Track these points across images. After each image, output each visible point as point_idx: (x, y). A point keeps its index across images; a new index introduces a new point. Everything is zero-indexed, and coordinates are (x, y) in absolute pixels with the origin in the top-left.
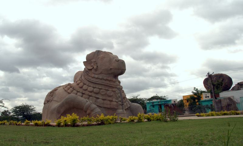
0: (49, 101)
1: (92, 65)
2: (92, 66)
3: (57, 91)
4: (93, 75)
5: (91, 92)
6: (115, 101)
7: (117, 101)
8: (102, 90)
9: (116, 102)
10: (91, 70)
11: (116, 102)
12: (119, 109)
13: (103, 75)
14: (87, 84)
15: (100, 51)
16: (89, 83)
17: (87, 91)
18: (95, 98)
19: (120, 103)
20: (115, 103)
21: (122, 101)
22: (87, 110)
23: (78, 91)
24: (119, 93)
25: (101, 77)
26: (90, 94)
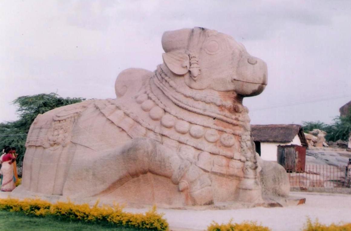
0: (58, 144)
1: (185, 65)
4: (189, 92)
5: (183, 133)
7: (243, 159)
8: (209, 131)
9: (240, 160)
10: (182, 76)
11: (240, 160)
12: (244, 177)
16: (178, 109)
17: (173, 129)
18: (193, 150)
20: (240, 164)
22: (180, 180)
23: (150, 127)
24: (248, 140)
26: (183, 138)
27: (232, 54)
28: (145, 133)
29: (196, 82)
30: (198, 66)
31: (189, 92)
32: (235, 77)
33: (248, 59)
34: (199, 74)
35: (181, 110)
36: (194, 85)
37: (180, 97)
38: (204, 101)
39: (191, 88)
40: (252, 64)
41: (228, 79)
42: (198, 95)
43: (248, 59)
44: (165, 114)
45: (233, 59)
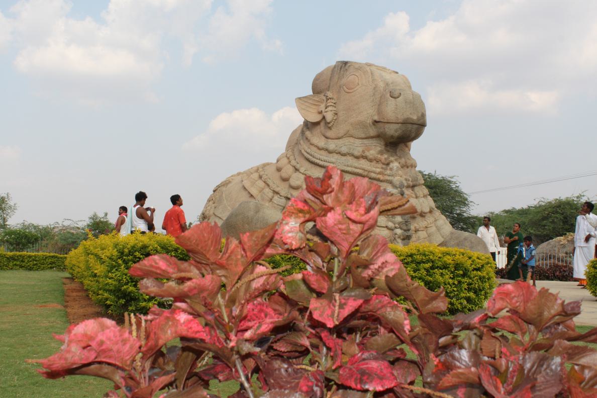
1: (320, 110)
2: (320, 113)
3: (229, 186)
4: (322, 143)
6: (384, 226)
7: (390, 225)
9: (386, 227)
10: (316, 124)
11: (386, 227)
13: (352, 140)
14: (302, 170)
15: (346, 63)
19: (399, 231)
21: (405, 228)
23: (277, 189)
25: (344, 150)
27: (374, 88)
28: (271, 197)
29: (331, 129)
30: (334, 109)
31: (322, 143)
32: (376, 118)
33: (391, 92)
34: (334, 118)
35: (313, 165)
36: (329, 133)
37: (313, 150)
38: (339, 153)
39: (327, 138)
40: (395, 98)
41: (368, 122)
42: (332, 145)
43: (391, 92)
44: (295, 172)
45: (374, 94)
